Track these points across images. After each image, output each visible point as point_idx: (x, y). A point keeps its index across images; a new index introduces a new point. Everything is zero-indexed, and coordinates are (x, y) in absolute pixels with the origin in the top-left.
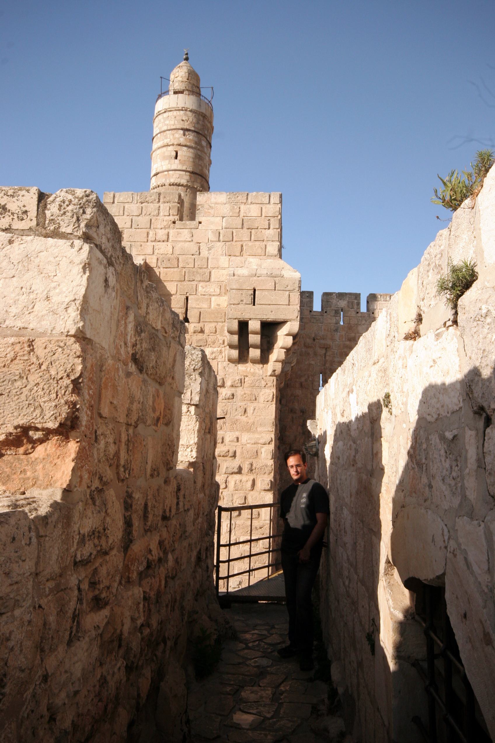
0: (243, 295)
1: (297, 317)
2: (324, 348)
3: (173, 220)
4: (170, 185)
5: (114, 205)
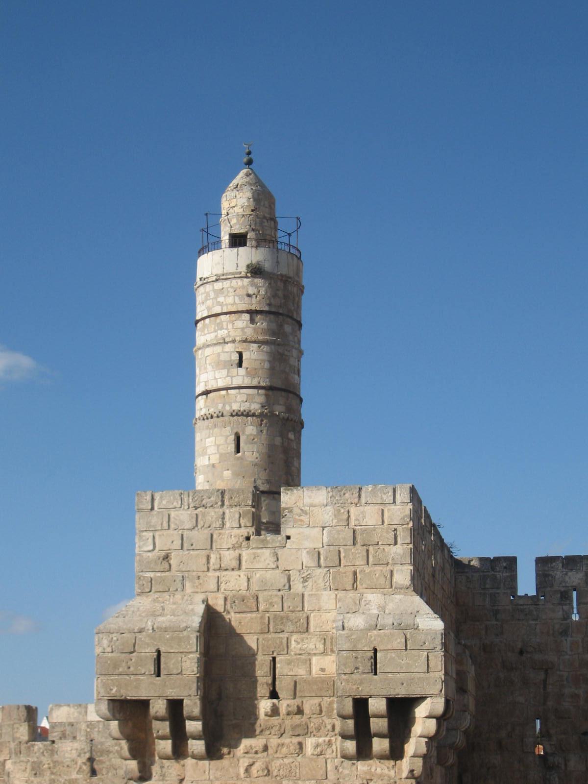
0: (359, 659)
1: (441, 691)
3: (246, 535)
4: (232, 415)
5: (154, 512)
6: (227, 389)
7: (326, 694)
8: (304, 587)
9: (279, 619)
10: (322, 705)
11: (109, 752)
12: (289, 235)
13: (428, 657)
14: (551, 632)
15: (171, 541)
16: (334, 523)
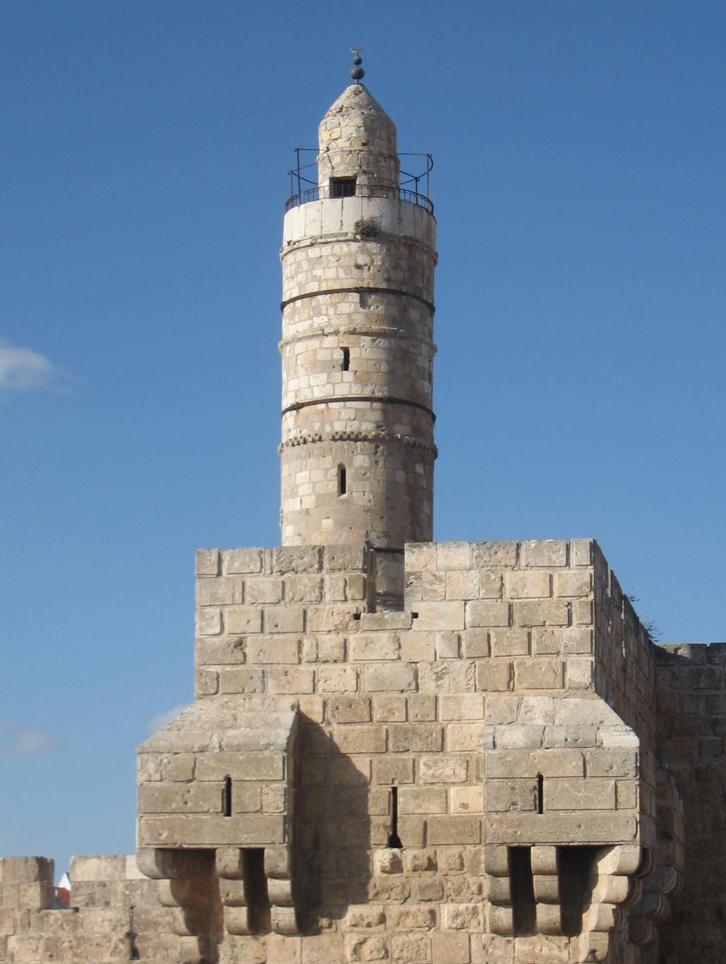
0: (517, 791)
1: (635, 836)
3: (354, 611)
4: (334, 439)
5: (222, 579)
6: (326, 401)
8: (438, 686)
9: (401, 734)
11: (156, 924)
12: (417, 179)
13: (616, 786)
15: (246, 621)
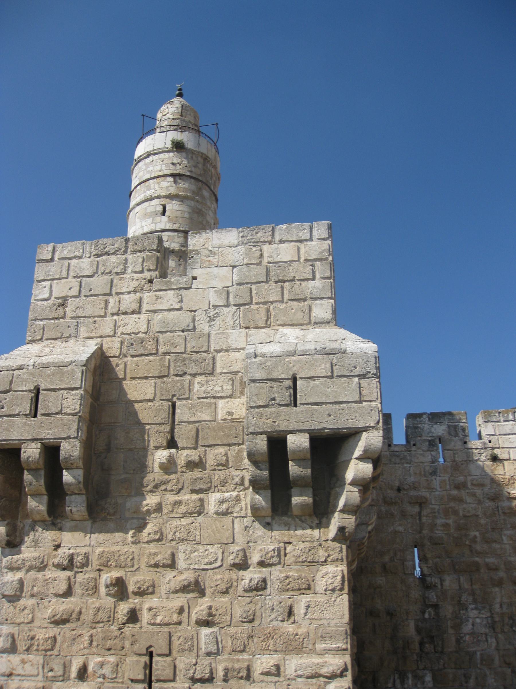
1: (378, 422)
2: (417, 503)
7: (235, 441)
8: (210, 326)
9: (181, 361)
10: (229, 455)
14: (423, 473)
15: (68, 288)
16: (245, 261)
